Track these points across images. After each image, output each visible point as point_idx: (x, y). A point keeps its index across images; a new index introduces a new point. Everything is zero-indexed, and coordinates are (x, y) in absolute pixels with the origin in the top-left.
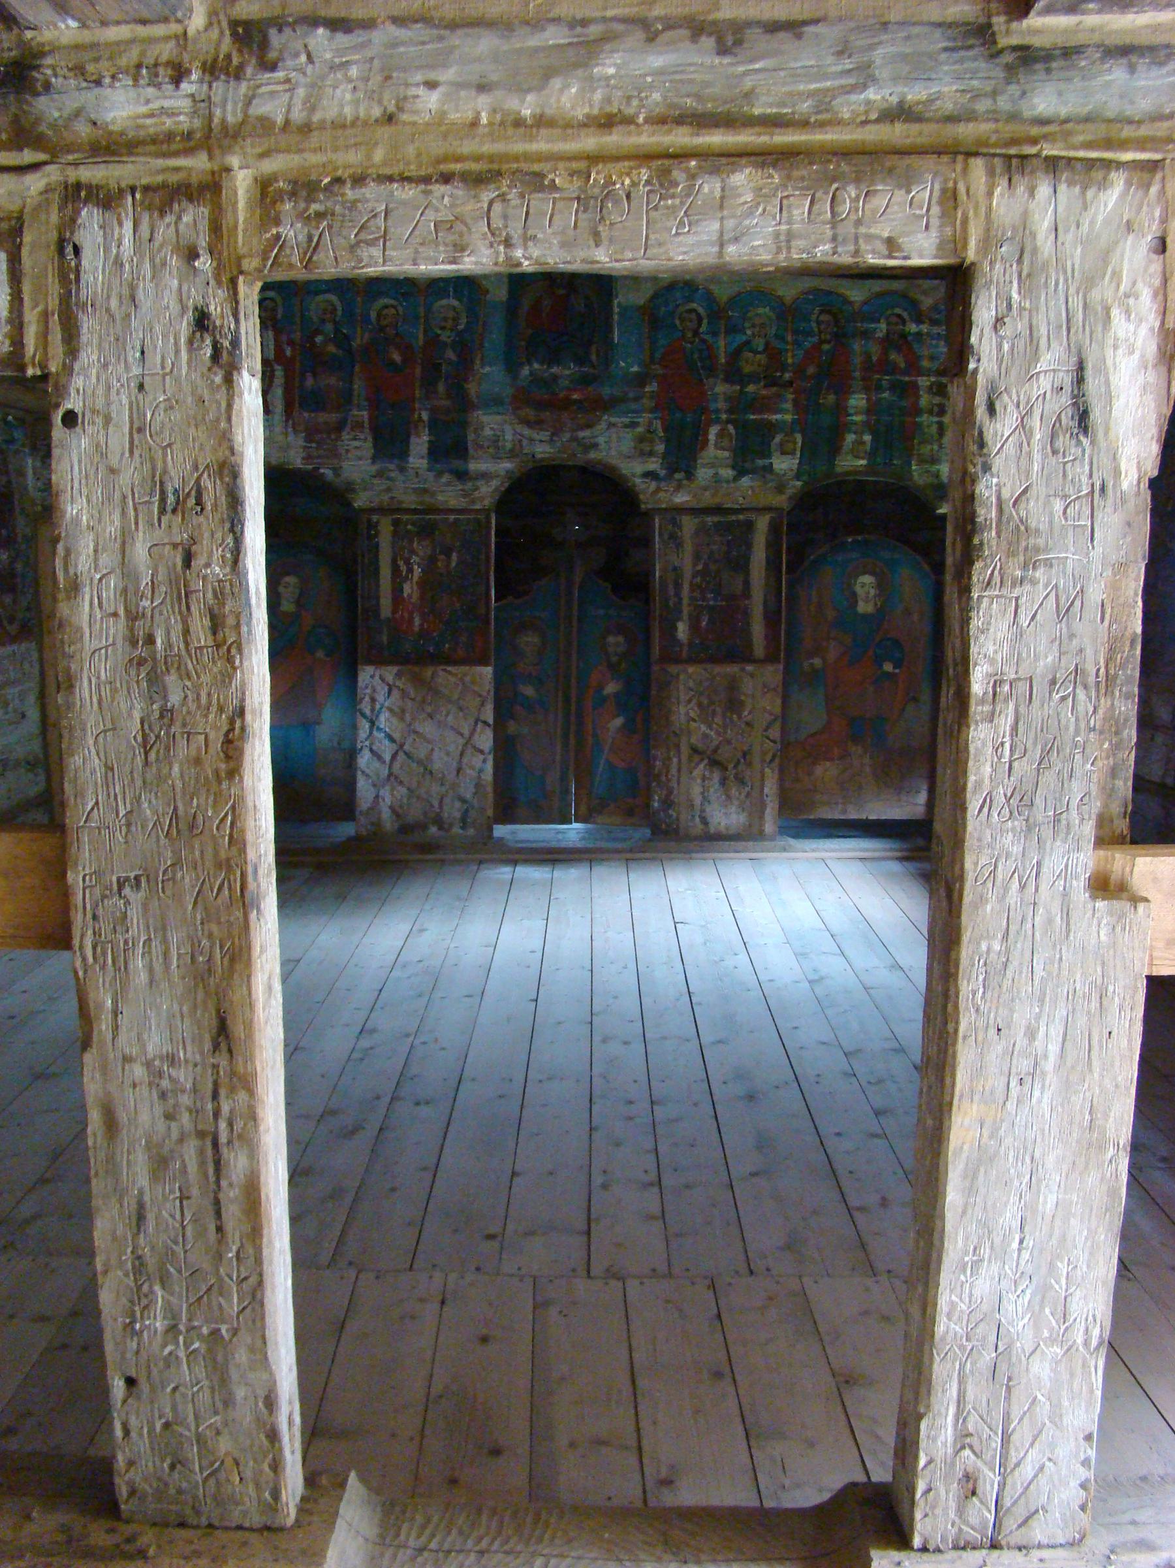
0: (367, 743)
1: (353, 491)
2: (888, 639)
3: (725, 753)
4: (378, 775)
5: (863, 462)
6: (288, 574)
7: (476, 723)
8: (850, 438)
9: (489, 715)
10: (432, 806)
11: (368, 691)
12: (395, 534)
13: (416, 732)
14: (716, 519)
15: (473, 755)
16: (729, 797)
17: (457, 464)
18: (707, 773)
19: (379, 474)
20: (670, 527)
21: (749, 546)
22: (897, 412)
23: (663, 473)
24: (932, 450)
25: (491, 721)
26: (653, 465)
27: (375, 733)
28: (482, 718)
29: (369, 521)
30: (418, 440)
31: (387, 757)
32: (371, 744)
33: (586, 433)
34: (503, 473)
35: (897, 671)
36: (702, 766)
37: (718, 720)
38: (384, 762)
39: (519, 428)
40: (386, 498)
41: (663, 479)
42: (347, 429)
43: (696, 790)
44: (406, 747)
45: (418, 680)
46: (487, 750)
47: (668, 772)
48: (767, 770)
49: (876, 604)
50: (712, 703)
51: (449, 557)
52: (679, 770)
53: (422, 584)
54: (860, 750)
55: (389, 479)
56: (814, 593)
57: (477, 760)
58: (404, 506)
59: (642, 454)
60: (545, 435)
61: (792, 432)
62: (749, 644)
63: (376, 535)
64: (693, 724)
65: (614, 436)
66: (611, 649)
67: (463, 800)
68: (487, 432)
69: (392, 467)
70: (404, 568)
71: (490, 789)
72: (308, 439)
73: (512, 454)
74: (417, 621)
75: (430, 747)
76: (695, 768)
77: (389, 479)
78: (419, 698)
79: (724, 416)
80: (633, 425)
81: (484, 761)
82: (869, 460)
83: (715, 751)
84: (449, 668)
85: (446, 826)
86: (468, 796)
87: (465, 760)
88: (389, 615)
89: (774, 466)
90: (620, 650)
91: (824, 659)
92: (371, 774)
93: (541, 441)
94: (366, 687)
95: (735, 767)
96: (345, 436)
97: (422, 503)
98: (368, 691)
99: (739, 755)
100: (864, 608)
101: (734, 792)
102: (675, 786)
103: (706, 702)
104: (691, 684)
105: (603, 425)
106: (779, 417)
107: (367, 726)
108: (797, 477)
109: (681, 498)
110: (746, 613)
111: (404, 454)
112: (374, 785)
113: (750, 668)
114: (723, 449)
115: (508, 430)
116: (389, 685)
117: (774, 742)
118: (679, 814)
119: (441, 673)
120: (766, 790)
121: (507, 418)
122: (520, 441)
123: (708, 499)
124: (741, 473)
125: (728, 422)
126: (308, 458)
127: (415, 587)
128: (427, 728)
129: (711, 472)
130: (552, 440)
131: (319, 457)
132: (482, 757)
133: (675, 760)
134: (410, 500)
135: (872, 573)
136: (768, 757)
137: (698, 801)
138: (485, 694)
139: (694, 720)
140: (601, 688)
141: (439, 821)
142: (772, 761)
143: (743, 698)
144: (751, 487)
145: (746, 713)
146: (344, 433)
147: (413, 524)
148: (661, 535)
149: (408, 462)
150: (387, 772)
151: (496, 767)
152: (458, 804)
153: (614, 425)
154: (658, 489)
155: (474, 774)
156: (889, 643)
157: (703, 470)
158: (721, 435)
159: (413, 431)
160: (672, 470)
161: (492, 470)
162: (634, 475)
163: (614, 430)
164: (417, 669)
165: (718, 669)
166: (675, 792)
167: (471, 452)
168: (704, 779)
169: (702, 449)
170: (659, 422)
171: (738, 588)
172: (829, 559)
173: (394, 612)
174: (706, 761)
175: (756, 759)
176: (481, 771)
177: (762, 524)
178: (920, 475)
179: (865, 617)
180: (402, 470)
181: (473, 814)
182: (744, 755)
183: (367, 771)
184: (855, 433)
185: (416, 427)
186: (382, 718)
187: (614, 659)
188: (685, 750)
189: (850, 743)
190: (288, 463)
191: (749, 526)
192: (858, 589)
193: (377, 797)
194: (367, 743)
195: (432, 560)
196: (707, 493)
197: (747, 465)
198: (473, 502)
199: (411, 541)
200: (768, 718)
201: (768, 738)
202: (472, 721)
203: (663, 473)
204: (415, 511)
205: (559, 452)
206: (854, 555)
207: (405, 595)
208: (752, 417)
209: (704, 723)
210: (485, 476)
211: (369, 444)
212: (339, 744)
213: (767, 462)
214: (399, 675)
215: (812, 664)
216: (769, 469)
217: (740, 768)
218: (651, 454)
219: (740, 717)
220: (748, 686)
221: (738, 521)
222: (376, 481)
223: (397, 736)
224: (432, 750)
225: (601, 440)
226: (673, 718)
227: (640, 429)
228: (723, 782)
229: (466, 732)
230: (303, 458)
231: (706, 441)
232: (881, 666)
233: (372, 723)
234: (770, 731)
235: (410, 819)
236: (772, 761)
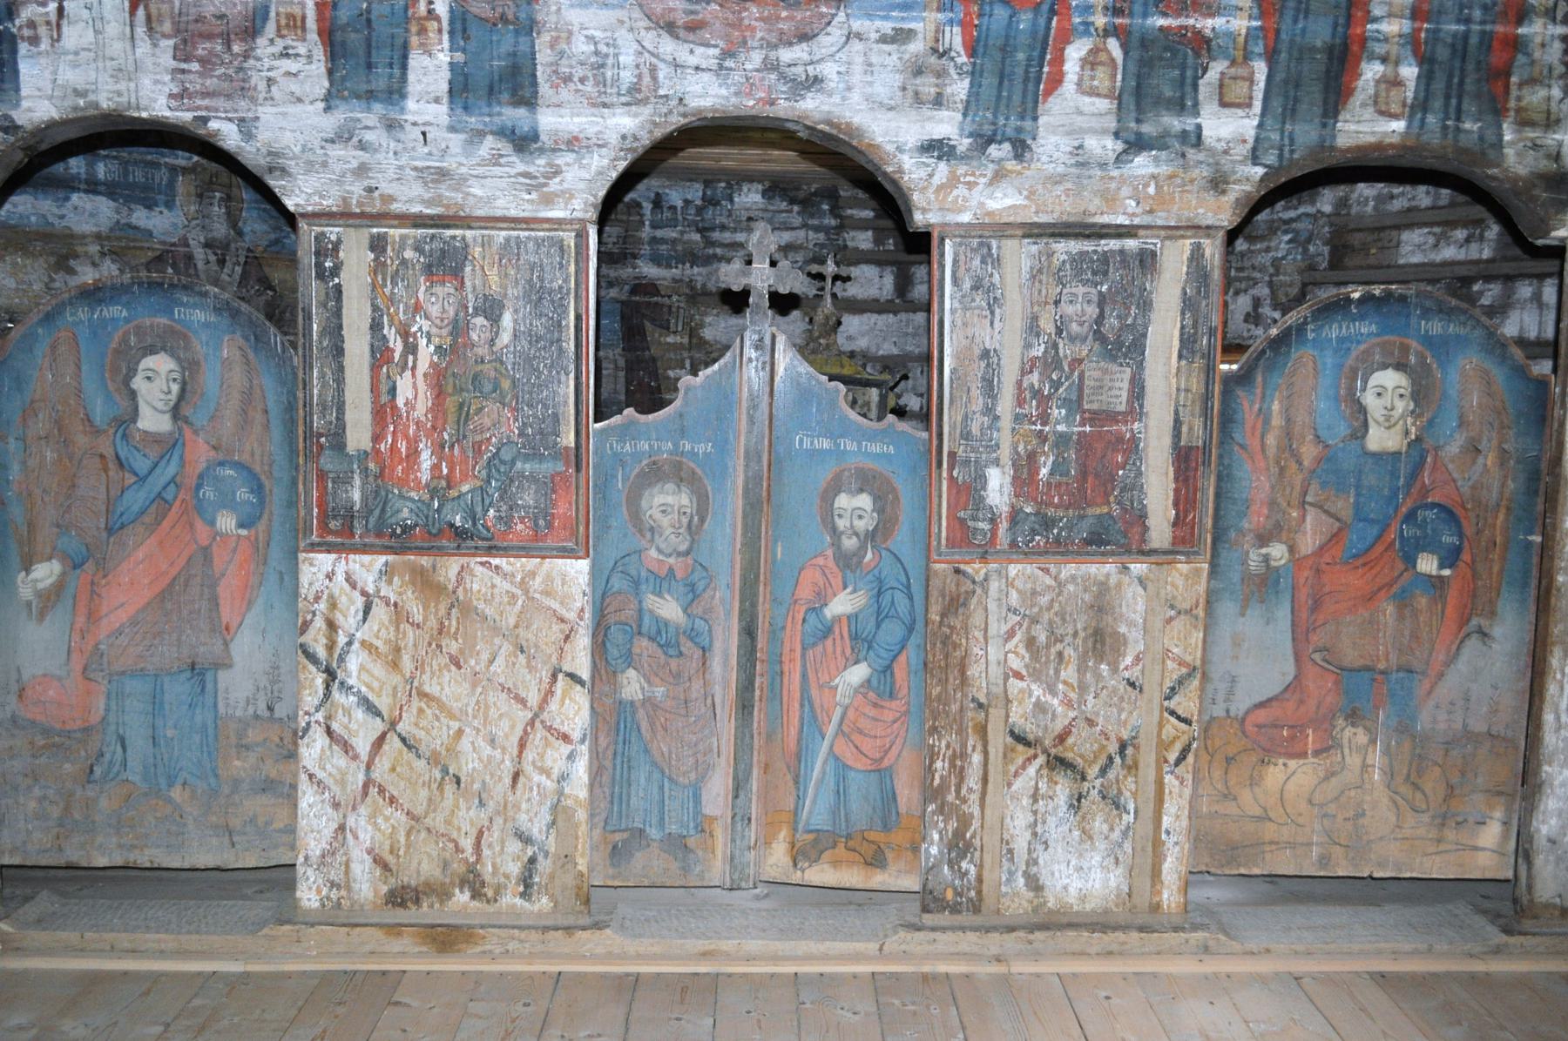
0: (320, 716)
1: (284, 171)
2: (1434, 505)
3: (1081, 746)
4: (342, 783)
5: (1399, 126)
6: (151, 350)
7: (554, 677)
8: (1371, 71)
9: (580, 659)
10: (458, 849)
11: (322, 606)
12: (378, 267)
13: (423, 695)
14: (1074, 246)
15: (547, 744)
16: (1087, 835)
17: (515, 115)
18: (1043, 786)
19: (343, 136)
20: (977, 262)
21: (1146, 306)
22: (1477, 14)
23: (963, 144)
24: (1549, 99)
25: (585, 675)
26: (946, 125)
27: (336, 695)
28: (566, 668)
29: (320, 238)
30: (426, 61)
31: (363, 746)
32: (329, 717)
33: (798, 53)
34: (614, 139)
35: (1446, 572)
36: (1032, 770)
37: (1069, 673)
38: (355, 757)
39: (649, 39)
40: (357, 189)
41: (964, 158)
42: (271, 28)
43: (1019, 824)
44: (400, 727)
45: (426, 584)
46: (576, 735)
47: (961, 779)
48: (1168, 778)
49: (1407, 433)
50: (1055, 639)
51: (495, 320)
52: (985, 780)
53: (439, 381)
54: (1362, 738)
55: (362, 146)
56: (1276, 406)
57: (556, 756)
58: (396, 207)
59: (918, 99)
60: (706, 56)
61: (1247, 57)
62: (1140, 518)
63: (336, 271)
64: (1015, 685)
65: (859, 59)
66: (842, 524)
67: (526, 839)
68: (581, 47)
69: (370, 119)
70: (397, 346)
71: (582, 815)
72: (183, 53)
73: (635, 96)
74: (426, 460)
75: (455, 725)
76: (1016, 775)
77: (362, 146)
78: (433, 623)
79: (1100, 21)
80: (901, 36)
81: (571, 757)
82: (1409, 127)
83: (1061, 738)
84: (495, 561)
85: (490, 894)
86: (537, 829)
87: (529, 755)
88: (366, 444)
89: (1205, 133)
90: (860, 525)
92: (329, 782)
93: (697, 68)
94: (317, 599)
95: (1103, 771)
96: (262, 45)
97: (428, 203)
98: (322, 606)
99: (1113, 748)
100: (1380, 439)
101: (1098, 825)
102: (976, 811)
103: (1042, 638)
104: (1014, 598)
105: (835, 35)
106: (1218, 22)
107: (320, 680)
108: (1255, 158)
109: (1004, 201)
110: (1132, 447)
111: (396, 93)
112: (336, 805)
113: (1137, 568)
114: (1094, 92)
115: (623, 36)
116: (364, 593)
118: (980, 867)
119: (479, 570)
120: (1166, 821)
121: (622, 14)
122: (653, 70)
123: (1059, 206)
124: (1137, 145)
125: (1107, 32)
126: (181, 96)
127: (421, 386)
128: (448, 686)
129: (1066, 144)
130: (721, 67)
131: (206, 94)
132: (566, 749)
133: (976, 758)
134: (411, 197)
135: (1400, 367)
136: (1172, 756)
137: (1021, 844)
138: (572, 616)
139: (1018, 676)
140: (822, 598)
141: (474, 883)
142: (1178, 762)
143: (1123, 629)
144: (1153, 177)
145: (1128, 660)
146: (261, 41)
147: (418, 249)
148: (955, 281)
149: (402, 110)
150: (361, 777)
151: (596, 773)
152: (514, 846)
153: (859, 36)
154: (953, 181)
155: (550, 785)
156: (1430, 514)
157: (1053, 139)
158: (1090, 62)
159: (414, 40)
160: (984, 140)
161: (591, 131)
162: (900, 149)
163: (857, 46)
164: (425, 561)
165: (1069, 570)
166: (976, 824)
167: (544, 88)
168: (1035, 797)
169: (1049, 92)
170: (956, 29)
171: (1119, 398)
172: (1310, 336)
173: (377, 438)
174: (1041, 760)
175: (1148, 759)
176: (563, 778)
177: (1175, 260)
178: (1518, 154)
179: (1378, 456)
180: (392, 126)
181: (544, 865)
182: (1123, 747)
183: (321, 775)
184: (1384, 60)
185: (423, 31)
186: (354, 662)
187: (850, 543)
188: (998, 739)
189: (1340, 722)
190: (129, 106)
191: (1147, 261)
192: (1369, 399)
193: (342, 828)
194: (320, 716)
195: (459, 329)
196: (1059, 190)
197: (1147, 129)
198: (548, 200)
199: (412, 288)
200: (1174, 671)
201: (1173, 713)
202: (545, 675)
203: (963, 144)
204: (418, 221)
205: (736, 94)
206: (1365, 328)
207: (400, 402)
208: (1161, 22)
209: (1036, 675)
210: (573, 143)
211: (319, 67)
212: (270, 708)
213: (1190, 123)
214: (387, 573)
216: (1195, 138)
217: (1111, 775)
218: (938, 101)
219: (1115, 670)
220: (1133, 604)
221: (1122, 252)
222: (336, 152)
223: (383, 703)
224: (460, 732)
225: (829, 70)
226: (974, 671)
227: (916, 47)
228: (1076, 802)
229: (533, 698)
230: (171, 96)
231: (1057, 80)
232: (1411, 561)
233: (331, 674)
234: (1177, 698)
235: (409, 878)
236: (1178, 762)
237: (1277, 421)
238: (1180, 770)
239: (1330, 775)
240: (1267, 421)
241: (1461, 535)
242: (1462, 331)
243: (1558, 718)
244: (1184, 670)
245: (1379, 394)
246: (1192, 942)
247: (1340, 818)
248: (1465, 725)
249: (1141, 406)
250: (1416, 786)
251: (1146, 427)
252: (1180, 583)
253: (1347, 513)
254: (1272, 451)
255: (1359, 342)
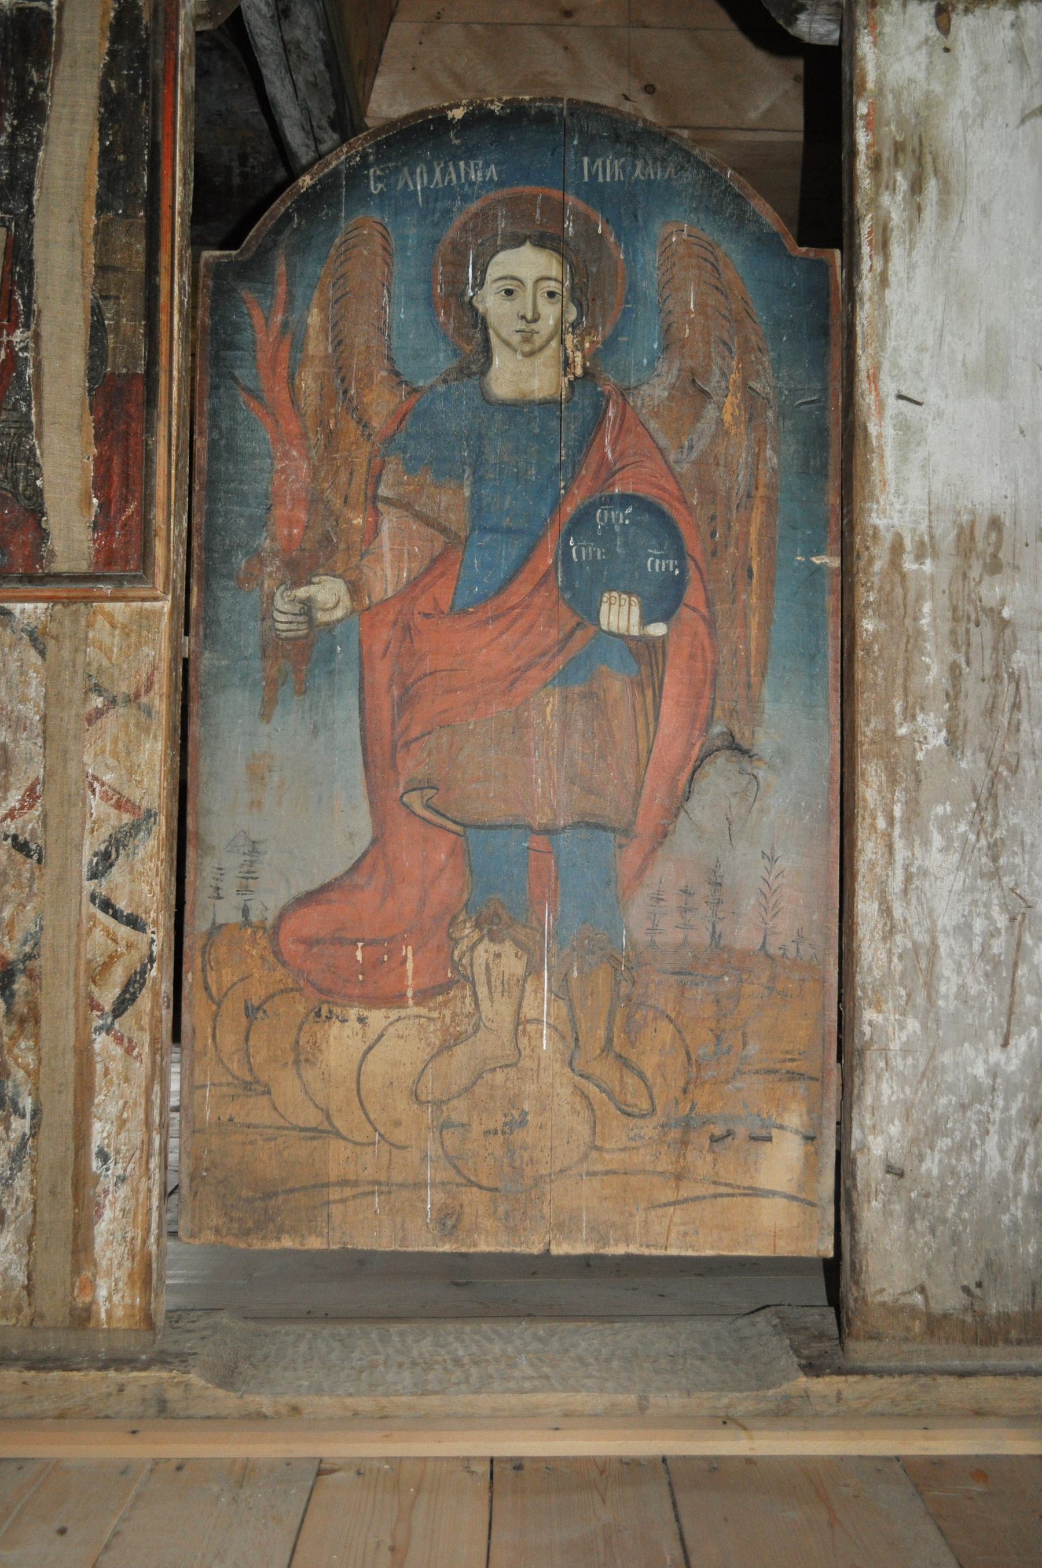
2: (625, 500)
35: (658, 629)
48: (101, 1042)
54: (513, 964)
56: (314, 319)
91: (355, 589)
117: (134, 922)
120: (99, 1132)
142: (121, 1007)
156: (621, 517)
201: (107, 906)
215: (307, 607)
236: (121, 1007)
237: (316, 346)
238: (125, 1024)
239: (450, 1042)
240: (299, 344)
241: (681, 555)
242: (656, 173)
243: (886, 911)
244: (127, 818)
245: (509, 292)
246: (132, 1390)
247: (476, 1130)
248: (715, 936)
249: (28, 300)
250: (624, 1062)
251: (37, 337)
252: (115, 641)
253: (457, 519)
254: (310, 402)
255: (465, 198)
